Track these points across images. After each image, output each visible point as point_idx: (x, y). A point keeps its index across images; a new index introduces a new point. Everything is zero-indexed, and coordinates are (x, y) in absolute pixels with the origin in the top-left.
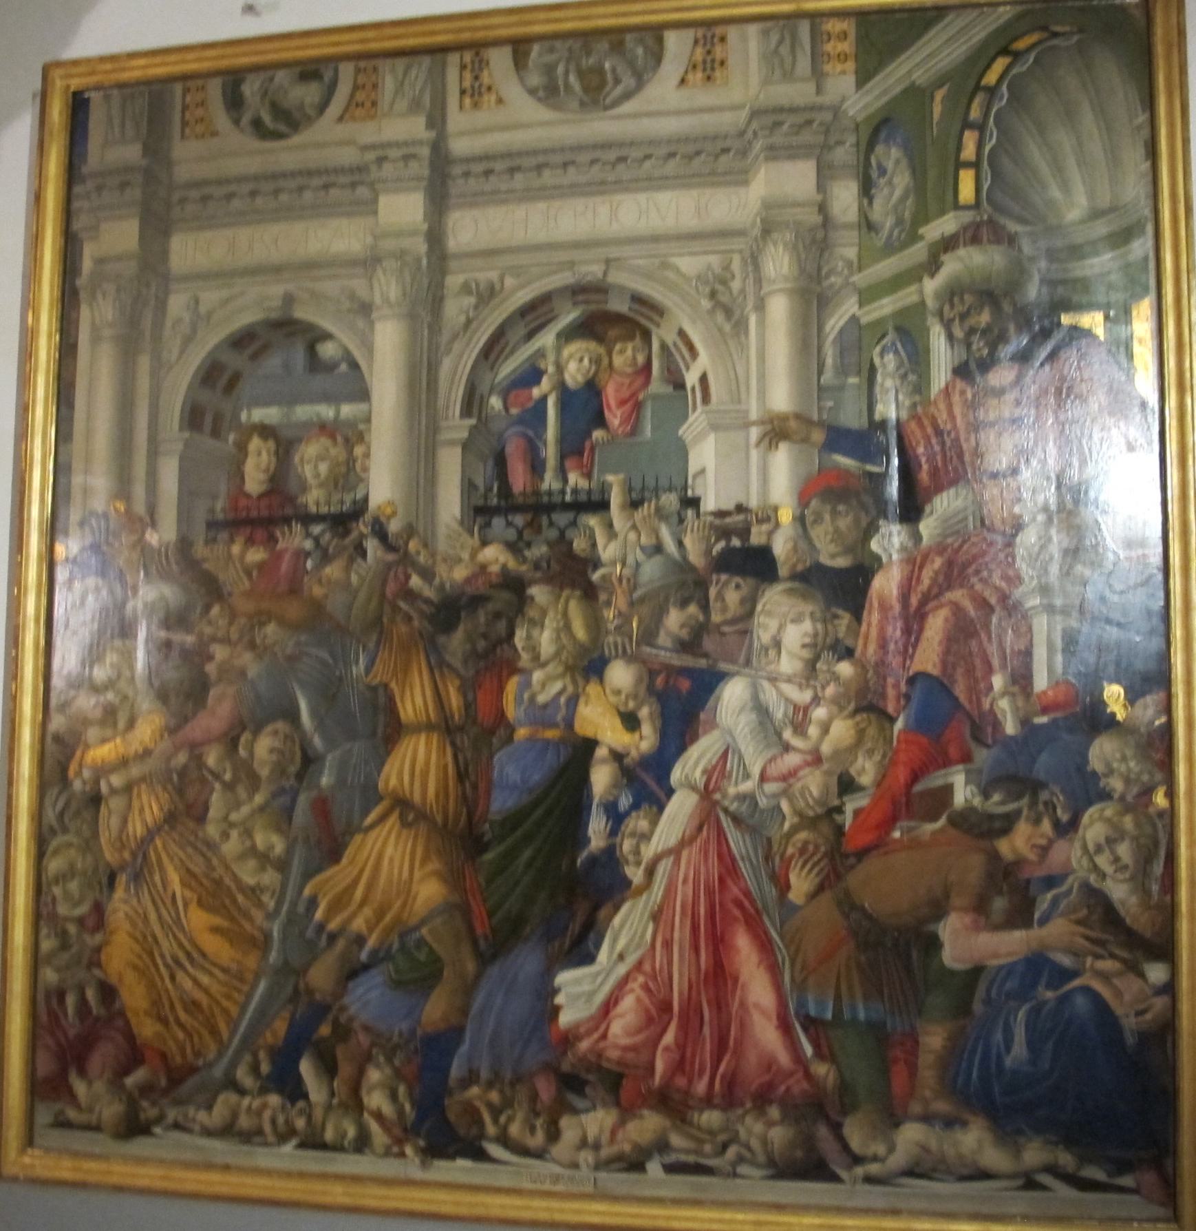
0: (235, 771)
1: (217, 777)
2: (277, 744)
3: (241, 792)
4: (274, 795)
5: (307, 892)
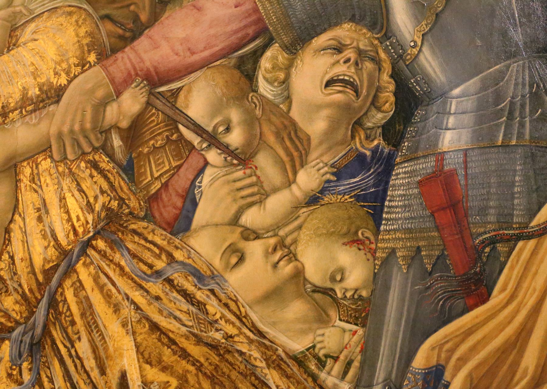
0: (250, 122)
1: (213, 140)
2: (341, 70)
3: (264, 162)
4: (340, 173)
5: (420, 360)
